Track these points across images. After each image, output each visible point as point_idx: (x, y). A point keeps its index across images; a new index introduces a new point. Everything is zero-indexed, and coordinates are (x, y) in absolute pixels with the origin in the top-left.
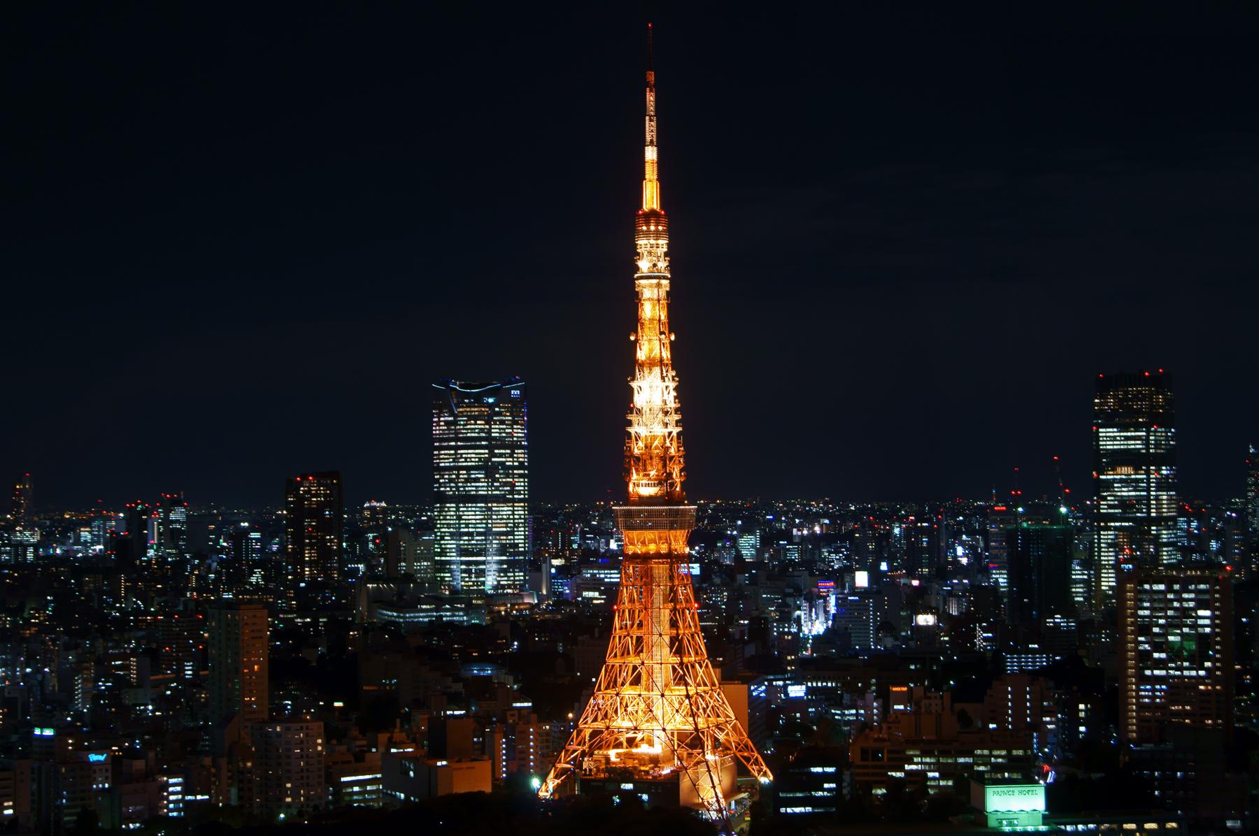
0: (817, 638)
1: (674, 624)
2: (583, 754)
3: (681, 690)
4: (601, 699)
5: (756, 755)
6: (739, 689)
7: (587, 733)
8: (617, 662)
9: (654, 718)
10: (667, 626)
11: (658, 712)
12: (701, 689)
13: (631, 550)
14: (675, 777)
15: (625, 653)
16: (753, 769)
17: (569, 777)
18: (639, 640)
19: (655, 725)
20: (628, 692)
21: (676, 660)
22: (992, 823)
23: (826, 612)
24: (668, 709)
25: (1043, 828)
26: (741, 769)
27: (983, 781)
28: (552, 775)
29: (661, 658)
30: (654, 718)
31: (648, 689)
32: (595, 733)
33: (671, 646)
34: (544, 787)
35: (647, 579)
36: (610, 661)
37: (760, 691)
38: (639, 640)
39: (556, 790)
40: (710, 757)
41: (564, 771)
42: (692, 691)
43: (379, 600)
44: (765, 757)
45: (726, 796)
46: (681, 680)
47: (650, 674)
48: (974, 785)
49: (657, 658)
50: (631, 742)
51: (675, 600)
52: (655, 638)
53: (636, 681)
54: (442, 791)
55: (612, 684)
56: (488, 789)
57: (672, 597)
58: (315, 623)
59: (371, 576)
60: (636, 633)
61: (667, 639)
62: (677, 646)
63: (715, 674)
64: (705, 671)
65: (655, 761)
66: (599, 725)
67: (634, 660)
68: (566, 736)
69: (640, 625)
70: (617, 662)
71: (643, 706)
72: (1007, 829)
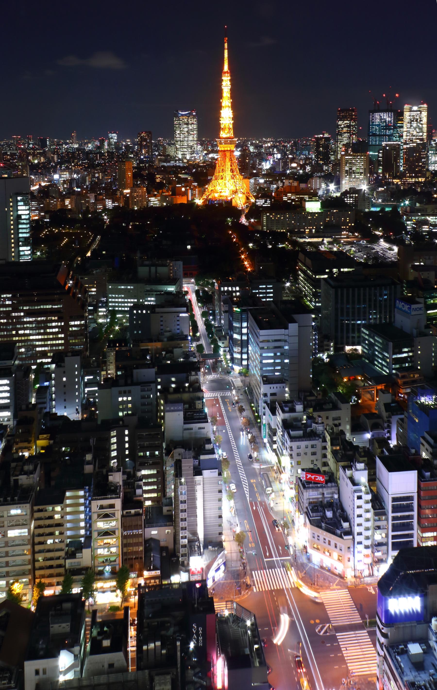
0: (267, 170)
1: (231, 166)
2: (209, 195)
3: (233, 180)
4: (214, 182)
5: (251, 195)
6: (246, 180)
7: (210, 190)
8: (217, 174)
9: (226, 187)
10: (230, 166)
11: (227, 185)
12: (238, 180)
13: (221, 149)
14: (231, 199)
15: (219, 172)
16: (250, 198)
17: (206, 200)
18: (223, 170)
19: (227, 189)
20: (220, 181)
21: (232, 174)
22: (307, 210)
23: (270, 163)
24: (230, 185)
25: (320, 211)
26: (247, 198)
27: (305, 201)
28: (201, 199)
29: (228, 174)
30: (226, 187)
31: (225, 180)
32: (211, 191)
33: (231, 171)
34: (199, 202)
35: (225, 156)
36: (216, 174)
37: (252, 181)
38: (223, 170)
39: (203, 203)
40: (240, 195)
41: (204, 199)
42: (235, 181)
43: (160, 160)
44: (253, 196)
45: (244, 204)
46: (233, 178)
47: (225, 177)
48: (303, 202)
49: (227, 174)
50: (221, 192)
51: (232, 160)
52: (227, 169)
53: (222, 179)
54: (174, 203)
55: (216, 179)
56: (186, 202)
57: (231, 160)
58: (145, 165)
59: (159, 155)
60: (222, 168)
61: (229, 169)
62: (232, 171)
63: (241, 177)
64: (239, 177)
65: (227, 197)
66: (213, 188)
67: (221, 174)
68: (205, 191)
69: (223, 166)
70: (217, 174)
71: (224, 184)
72: (311, 212)
